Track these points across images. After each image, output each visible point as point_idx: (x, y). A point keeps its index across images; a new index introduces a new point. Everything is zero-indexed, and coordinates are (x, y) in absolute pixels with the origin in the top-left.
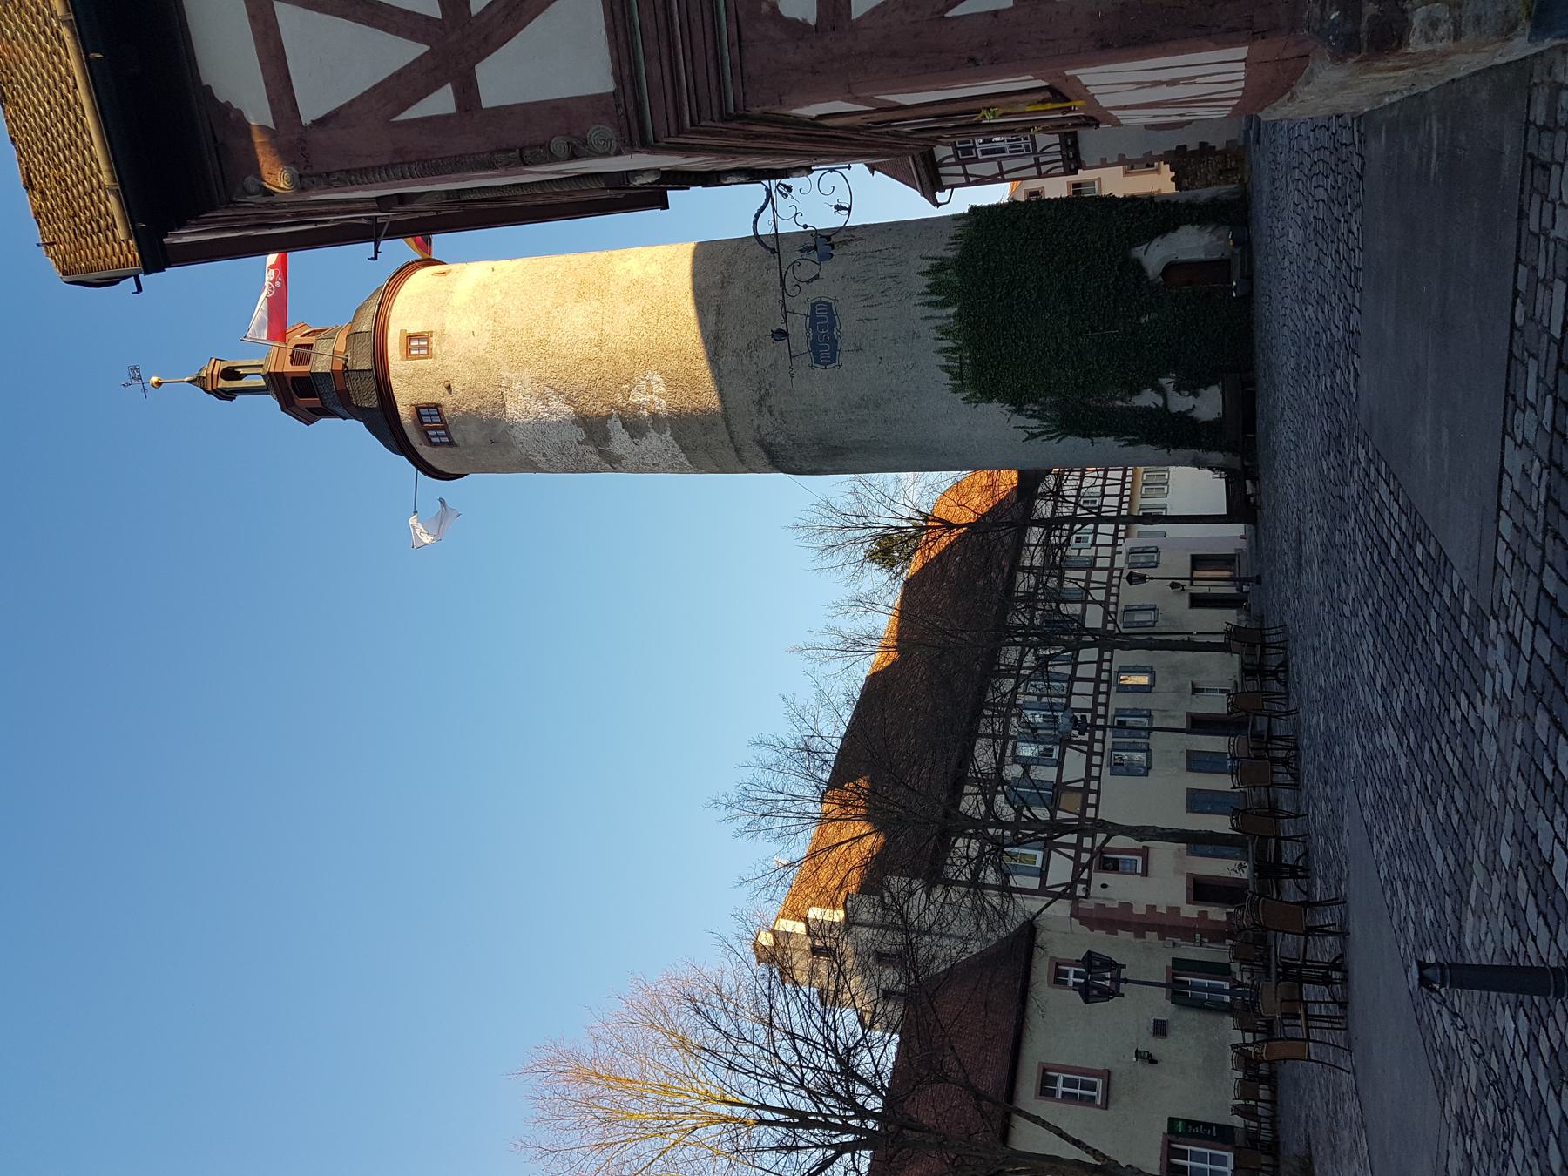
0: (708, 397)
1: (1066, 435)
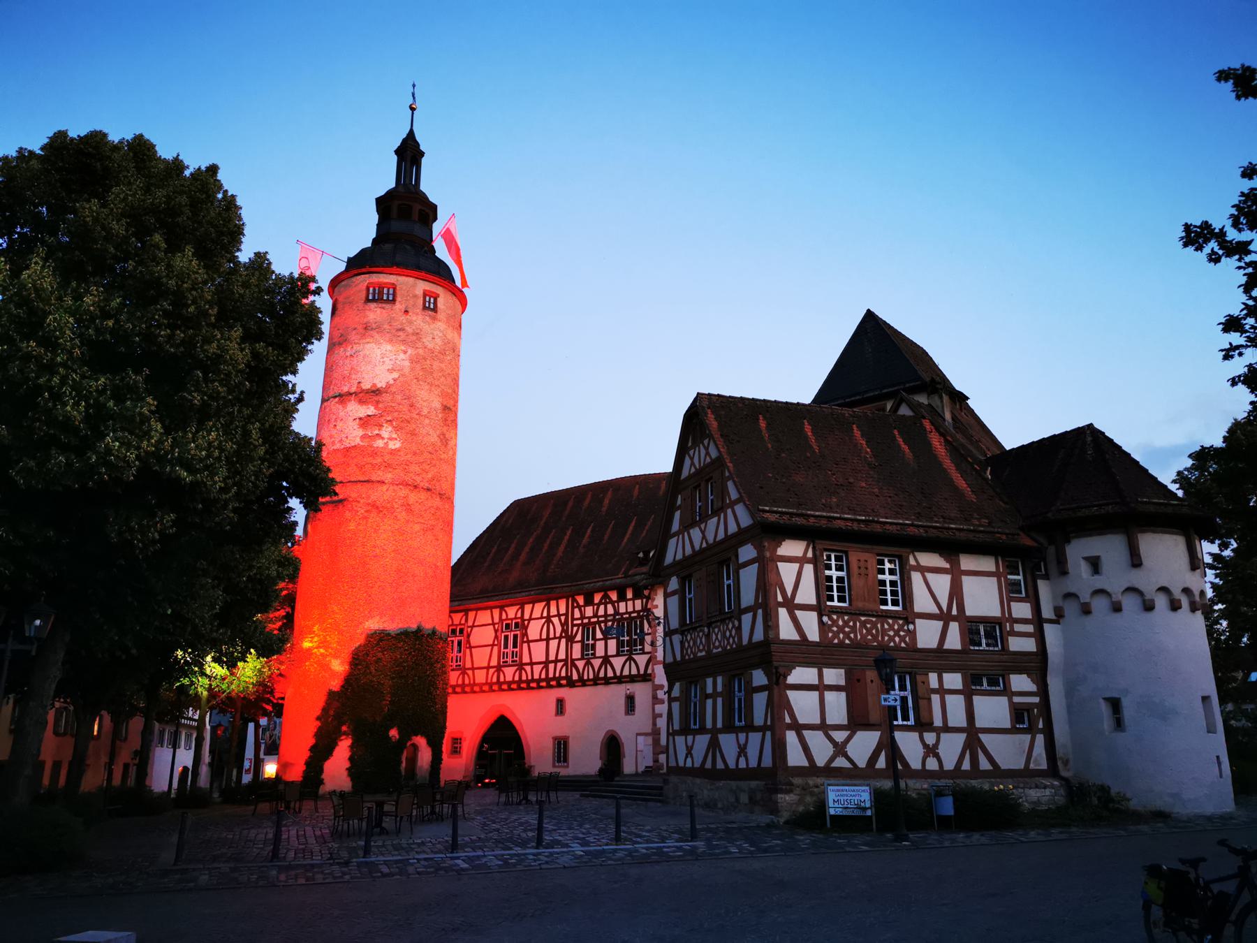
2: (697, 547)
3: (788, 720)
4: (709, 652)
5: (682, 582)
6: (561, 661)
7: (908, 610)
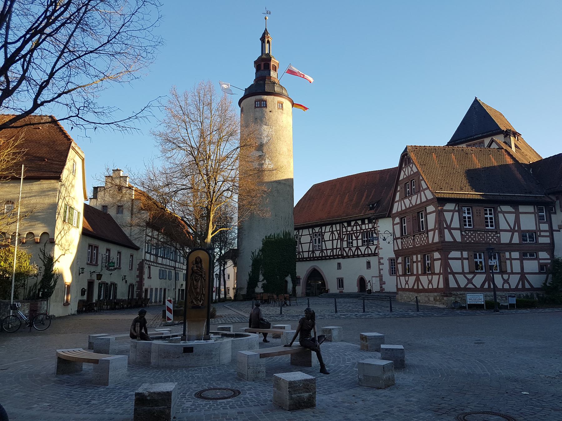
0: (267, 178)
1: (253, 261)
2: (408, 207)
3: (449, 271)
4: (414, 246)
5: (401, 219)
6: (338, 248)
7: (497, 228)
